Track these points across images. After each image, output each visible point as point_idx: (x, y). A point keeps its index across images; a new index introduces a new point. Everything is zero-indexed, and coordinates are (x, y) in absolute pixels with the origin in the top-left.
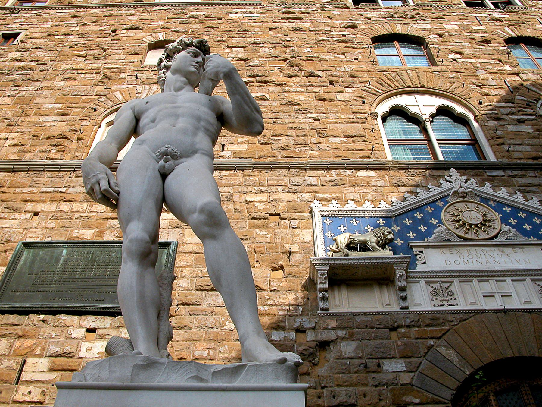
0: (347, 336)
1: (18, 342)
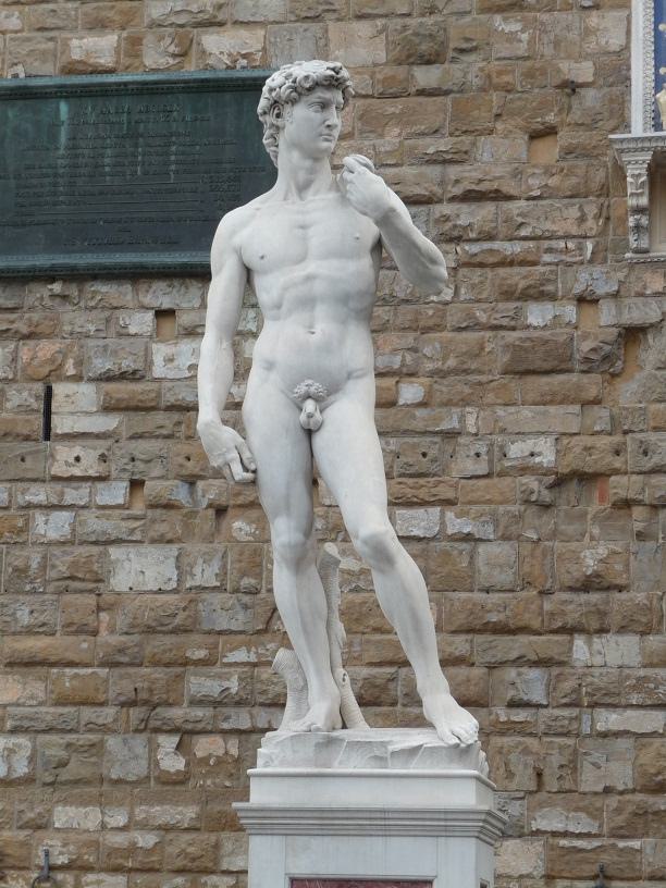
1: (26, 348)
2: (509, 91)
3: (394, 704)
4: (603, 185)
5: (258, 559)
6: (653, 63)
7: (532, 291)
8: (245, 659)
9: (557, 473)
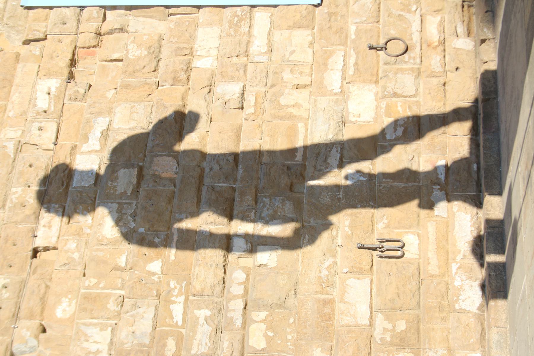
3: (234, 189)
8: (182, 305)
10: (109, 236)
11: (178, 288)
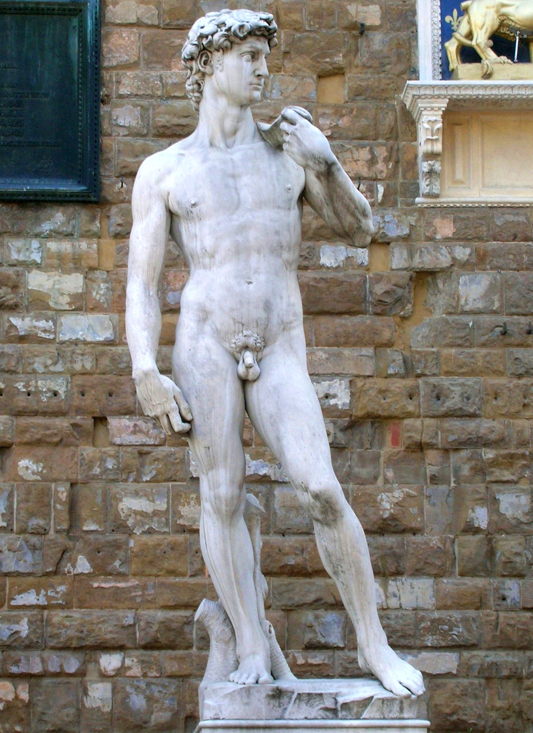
0: (474, 260)
2: (296, 30)
3: (189, 647)
4: (392, 129)
5: (46, 500)
6: (439, 11)
7: (325, 232)
9: (351, 416)
10: (121, 506)
11: (56, 596)
